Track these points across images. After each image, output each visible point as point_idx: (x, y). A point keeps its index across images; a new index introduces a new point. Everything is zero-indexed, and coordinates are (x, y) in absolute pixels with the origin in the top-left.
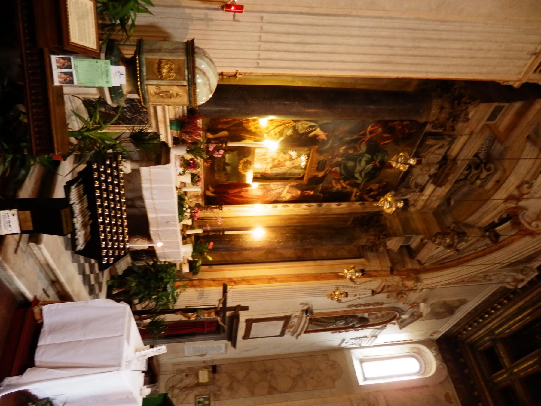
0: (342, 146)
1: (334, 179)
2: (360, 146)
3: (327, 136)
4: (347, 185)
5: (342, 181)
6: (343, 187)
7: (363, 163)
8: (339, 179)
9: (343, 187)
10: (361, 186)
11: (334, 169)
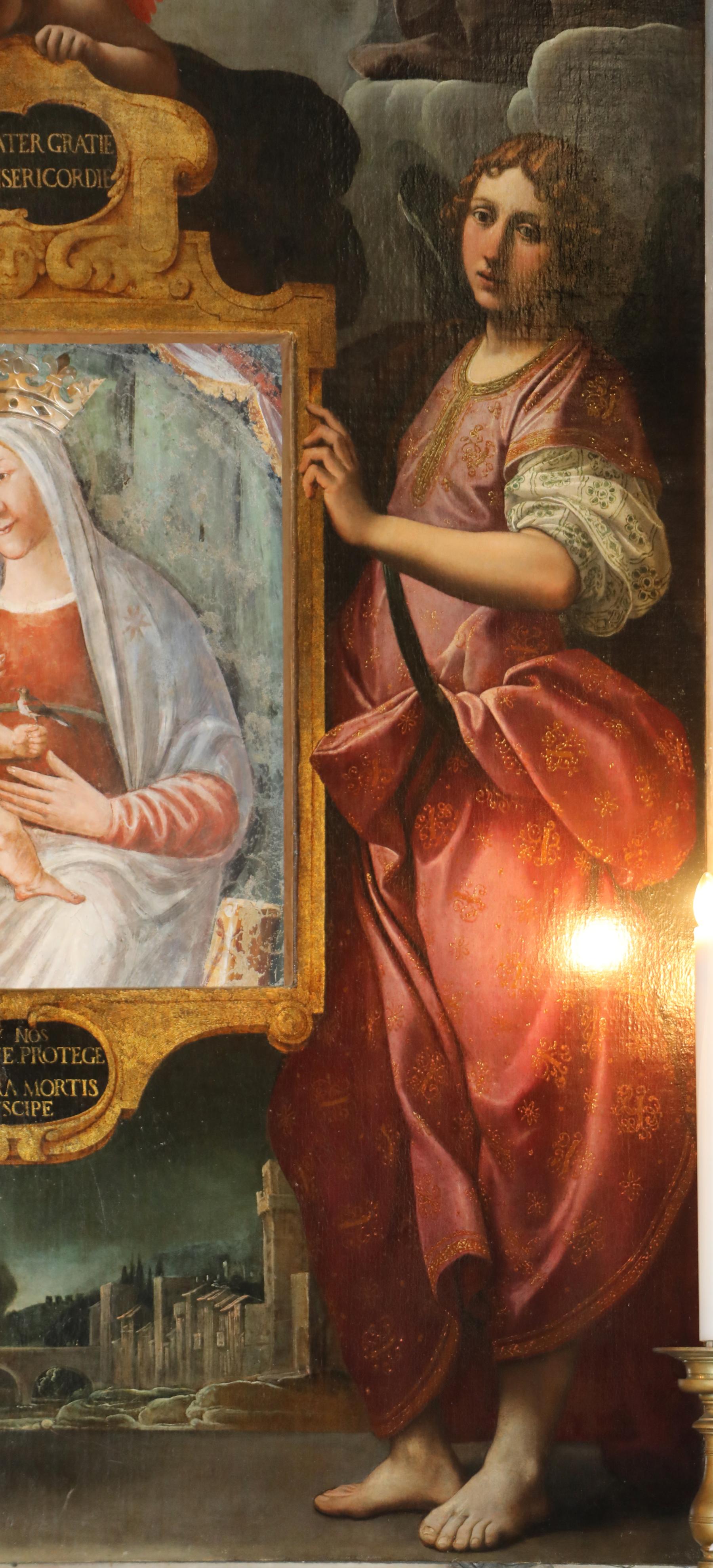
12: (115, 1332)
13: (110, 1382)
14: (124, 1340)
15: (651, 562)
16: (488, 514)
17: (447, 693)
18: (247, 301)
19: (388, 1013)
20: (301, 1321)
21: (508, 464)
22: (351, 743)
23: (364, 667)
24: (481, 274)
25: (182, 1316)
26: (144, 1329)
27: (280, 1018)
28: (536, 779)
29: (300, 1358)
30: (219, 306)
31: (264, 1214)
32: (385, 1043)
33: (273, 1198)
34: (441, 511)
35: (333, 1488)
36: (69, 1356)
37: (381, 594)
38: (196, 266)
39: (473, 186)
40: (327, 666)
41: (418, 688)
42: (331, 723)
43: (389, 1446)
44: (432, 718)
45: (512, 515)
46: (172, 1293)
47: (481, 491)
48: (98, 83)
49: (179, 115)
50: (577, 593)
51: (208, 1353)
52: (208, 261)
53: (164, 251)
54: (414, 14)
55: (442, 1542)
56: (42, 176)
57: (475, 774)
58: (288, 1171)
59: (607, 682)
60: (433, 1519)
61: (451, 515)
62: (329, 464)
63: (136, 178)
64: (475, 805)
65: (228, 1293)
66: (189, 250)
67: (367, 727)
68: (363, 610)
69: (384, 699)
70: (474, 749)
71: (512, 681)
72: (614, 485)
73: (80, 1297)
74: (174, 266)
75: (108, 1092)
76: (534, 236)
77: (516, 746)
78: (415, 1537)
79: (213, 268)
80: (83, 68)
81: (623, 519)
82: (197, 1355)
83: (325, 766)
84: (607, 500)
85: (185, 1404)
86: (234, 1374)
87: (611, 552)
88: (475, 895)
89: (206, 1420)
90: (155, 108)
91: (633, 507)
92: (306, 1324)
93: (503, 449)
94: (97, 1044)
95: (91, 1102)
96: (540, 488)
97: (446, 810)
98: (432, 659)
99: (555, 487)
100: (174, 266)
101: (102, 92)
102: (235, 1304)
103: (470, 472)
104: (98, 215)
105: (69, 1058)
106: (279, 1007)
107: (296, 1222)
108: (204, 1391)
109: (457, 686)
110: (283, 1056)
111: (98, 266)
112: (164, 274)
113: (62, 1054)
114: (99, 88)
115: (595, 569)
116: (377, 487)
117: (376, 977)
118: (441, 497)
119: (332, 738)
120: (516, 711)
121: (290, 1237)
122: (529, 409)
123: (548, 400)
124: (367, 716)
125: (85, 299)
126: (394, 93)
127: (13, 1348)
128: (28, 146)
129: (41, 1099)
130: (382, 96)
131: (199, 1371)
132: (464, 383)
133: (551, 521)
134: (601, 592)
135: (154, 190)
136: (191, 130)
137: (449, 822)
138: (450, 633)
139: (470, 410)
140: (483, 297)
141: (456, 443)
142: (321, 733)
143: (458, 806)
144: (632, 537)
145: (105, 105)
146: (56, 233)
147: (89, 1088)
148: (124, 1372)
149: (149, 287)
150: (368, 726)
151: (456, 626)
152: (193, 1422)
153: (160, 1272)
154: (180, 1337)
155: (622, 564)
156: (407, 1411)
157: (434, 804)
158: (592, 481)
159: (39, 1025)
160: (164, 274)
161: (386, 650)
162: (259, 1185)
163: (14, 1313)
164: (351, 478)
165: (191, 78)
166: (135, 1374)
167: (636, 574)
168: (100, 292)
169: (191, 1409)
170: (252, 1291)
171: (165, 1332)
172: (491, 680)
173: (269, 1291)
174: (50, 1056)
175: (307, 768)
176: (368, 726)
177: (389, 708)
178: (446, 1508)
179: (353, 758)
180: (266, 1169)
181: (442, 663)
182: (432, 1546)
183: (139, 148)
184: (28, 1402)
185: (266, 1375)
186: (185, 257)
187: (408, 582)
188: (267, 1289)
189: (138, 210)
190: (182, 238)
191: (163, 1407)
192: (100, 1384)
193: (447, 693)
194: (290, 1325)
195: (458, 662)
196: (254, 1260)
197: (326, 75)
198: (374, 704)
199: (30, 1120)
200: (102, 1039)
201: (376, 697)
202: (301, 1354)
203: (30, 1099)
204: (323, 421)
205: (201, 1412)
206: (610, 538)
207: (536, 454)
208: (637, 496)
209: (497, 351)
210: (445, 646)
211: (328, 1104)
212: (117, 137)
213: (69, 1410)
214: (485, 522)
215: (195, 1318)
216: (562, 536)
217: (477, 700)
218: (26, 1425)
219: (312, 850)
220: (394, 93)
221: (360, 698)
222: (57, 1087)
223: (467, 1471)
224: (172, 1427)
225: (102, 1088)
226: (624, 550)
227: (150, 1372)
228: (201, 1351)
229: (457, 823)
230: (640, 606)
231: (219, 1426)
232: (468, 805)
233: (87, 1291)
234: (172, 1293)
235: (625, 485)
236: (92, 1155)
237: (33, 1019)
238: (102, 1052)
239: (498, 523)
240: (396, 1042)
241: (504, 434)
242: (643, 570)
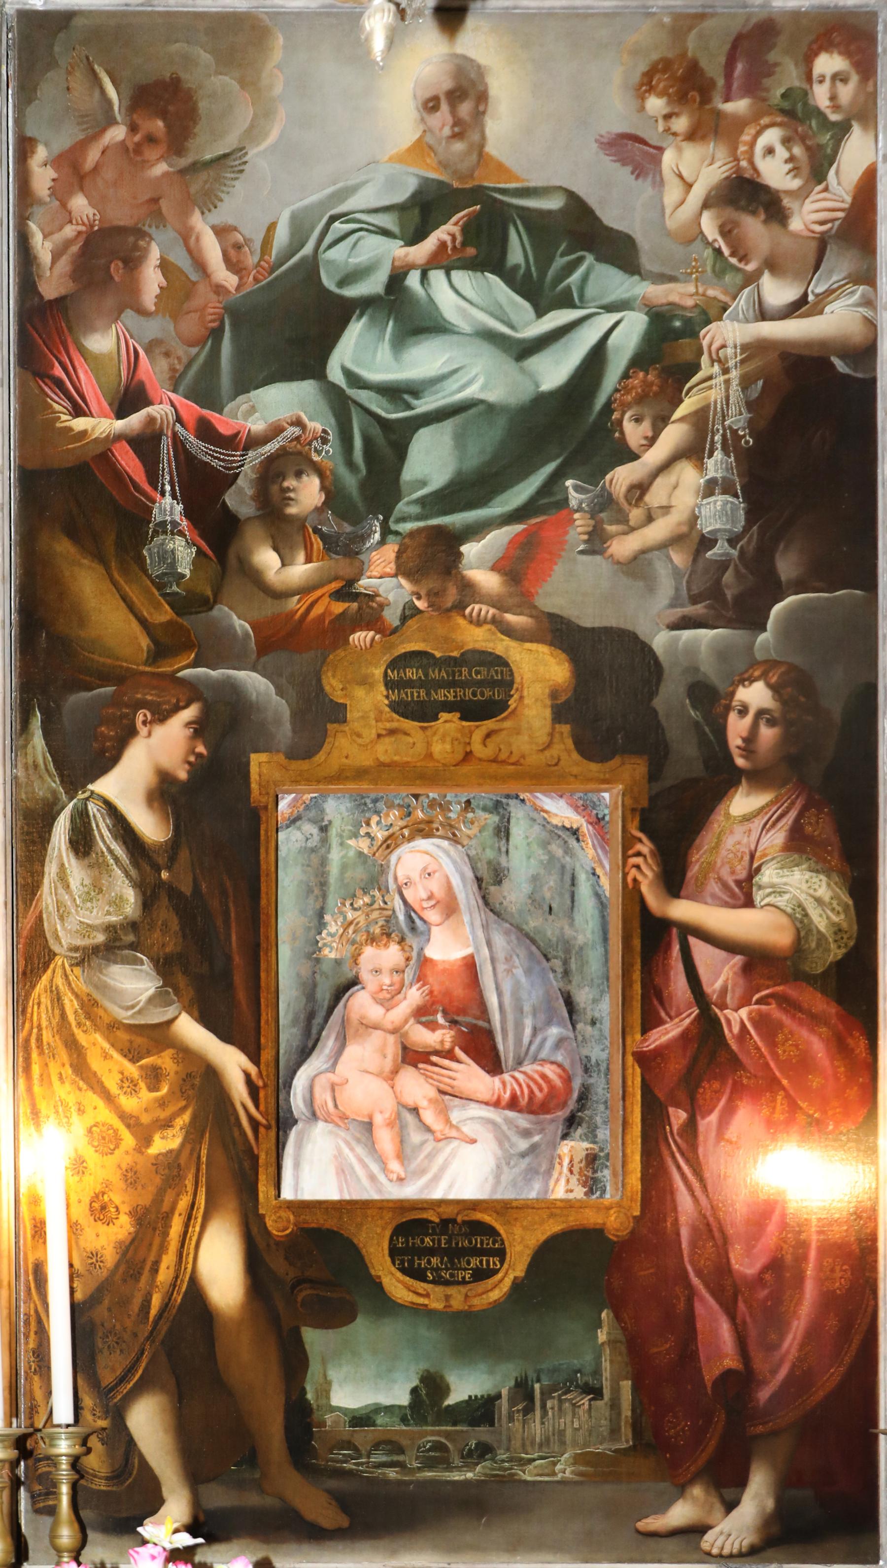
0: (254, 577)
1: (596, 542)
2: (254, 442)
3: (161, 716)
4: (661, 422)
5: (622, 477)
6: (694, 451)
7: (424, 360)
8: (605, 503)
9: (694, 451)
10: (680, 294)
11: (487, 580)
12: (511, 1419)
13: (508, 1450)
14: (516, 1423)
15: (845, 925)
16: (742, 898)
17: (717, 1011)
18: (594, 767)
19: (680, 1215)
20: (626, 1412)
21: (755, 865)
22: (657, 1043)
23: (665, 994)
24: (739, 747)
25: (552, 1408)
26: (529, 1416)
27: (613, 1218)
28: (772, 1064)
29: (626, 1435)
30: (575, 770)
31: (603, 1344)
32: (678, 1234)
33: (609, 1333)
34: (714, 896)
35: (646, 1517)
36: (482, 1433)
37: (676, 949)
38: (562, 746)
39: (732, 694)
40: (643, 995)
41: (699, 1008)
42: (645, 1030)
43: (681, 1490)
44: (708, 1025)
45: (758, 897)
46: (546, 1394)
47: (738, 883)
48: (503, 637)
49: (552, 655)
50: (799, 948)
51: (569, 1432)
52: (570, 743)
53: (542, 737)
54: (695, 591)
55: (715, 1551)
56: (469, 692)
57: (735, 1062)
58: (617, 1316)
59: (818, 1002)
60: (709, 1536)
61: (719, 898)
62: (644, 867)
63: (525, 693)
64: (735, 1083)
65: (581, 1393)
66: (557, 735)
67: (667, 1033)
68: (665, 959)
69: (677, 1016)
70: (734, 1046)
71: (758, 1002)
72: (822, 877)
73: (489, 1395)
74: (548, 746)
75: (506, 1266)
76: (771, 723)
77: (760, 1044)
78: (698, 1548)
79: (572, 747)
80: (493, 628)
81: (827, 899)
82: (562, 1433)
83: (642, 1058)
84: (816, 887)
85: (555, 1464)
86: (586, 1445)
87: (820, 920)
88: (734, 1139)
89: (568, 1474)
90: (537, 651)
91: (833, 891)
92: (629, 1413)
93: (752, 857)
94: (499, 1235)
95: (496, 1272)
96: (776, 880)
97: (716, 1085)
98: (708, 989)
99: (784, 880)
100: (548, 746)
101: (505, 643)
102: (585, 1401)
103: (731, 871)
104: (503, 715)
105: (482, 1243)
106: (612, 1212)
107: (623, 1348)
108: (566, 1456)
109: (723, 1006)
110: (615, 1243)
111: (502, 747)
112: (542, 751)
113: (477, 1241)
114: (502, 640)
115: (810, 930)
116: (674, 882)
117: (672, 1192)
118: (714, 887)
119: (645, 1040)
120: (760, 1021)
121: (619, 1358)
122: (768, 831)
123: (780, 825)
124: (667, 1026)
125: (494, 765)
126: (684, 638)
127: (449, 1428)
128: (461, 675)
129: (465, 1269)
130: (678, 639)
131: (563, 1443)
132: (728, 815)
133: (781, 901)
134: (813, 945)
135: (537, 700)
136: (558, 664)
137: (718, 1093)
138: (718, 972)
139: (732, 832)
140: (740, 762)
141: (723, 853)
142: (638, 1037)
143: (723, 1083)
144: (833, 910)
145: (507, 649)
146: (477, 727)
147: (494, 1263)
148: (516, 1443)
149: (535, 759)
150: (667, 1033)
151: (723, 968)
152: (560, 1475)
153: (538, 1381)
154: (551, 1422)
155: (826, 927)
156: (693, 1469)
157: (709, 1081)
158: (808, 875)
159: (464, 1222)
160: (542, 751)
161: (679, 984)
162: (599, 1325)
163: (449, 1406)
164: (657, 876)
165: (559, 632)
166: (523, 1445)
167: (835, 933)
168: (503, 762)
169: (558, 1467)
170: (596, 1392)
171: (542, 1418)
172: (745, 1002)
173: (607, 1393)
174: (470, 1242)
175: (630, 1059)
176: (667, 1033)
177: (681, 1021)
178: (717, 1530)
179: (659, 1053)
180: (604, 1315)
181: (714, 991)
182: (709, 1554)
183: (527, 676)
184: (457, 1462)
185: (605, 1446)
186: (555, 740)
187: (692, 940)
188: (605, 1391)
189: (527, 712)
190: (553, 729)
191: (541, 1465)
192: (502, 1451)
193: (717, 1011)
194: (619, 1414)
195: (724, 991)
196: (597, 1372)
197: (642, 630)
198: (671, 1018)
199: (458, 1283)
200: (502, 1232)
201: (673, 1013)
202: (626, 1432)
203: (458, 1269)
204: (640, 841)
205: (565, 1469)
206: (819, 911)
207: (773, 859)
208: (836, 884)
209: (748, 794)
210: (716, 981)
211: (642, 1273)
212: (514, 668)
213: (483, 1467)
214: (741, 902)
215: (560, 1409)
216: (789, 910)
217: (735, 1014)
218: (456, 1476)
219: (632, 1112)
220: (684, 638)
221: (663, 1014)
222: (474, 1262)
223: (730, 1506)
224: (547, 1479)
225: (502, 1262)
226: (828, 918)
227: (533, 1443)
228: (564, 1430)
229: (723, 1093)
230: (836, 953)
231: (577, 1478)
232: (730, 1081)
233: (493, 1393)
234: (546, 1394)
235: (828, 877)
236: (496, 1304)
237: (459, 1219)
238: (502, 1240)
239: (749, 903)
240: (685, 1233)
241: (753, 847)
242: (840, 930)
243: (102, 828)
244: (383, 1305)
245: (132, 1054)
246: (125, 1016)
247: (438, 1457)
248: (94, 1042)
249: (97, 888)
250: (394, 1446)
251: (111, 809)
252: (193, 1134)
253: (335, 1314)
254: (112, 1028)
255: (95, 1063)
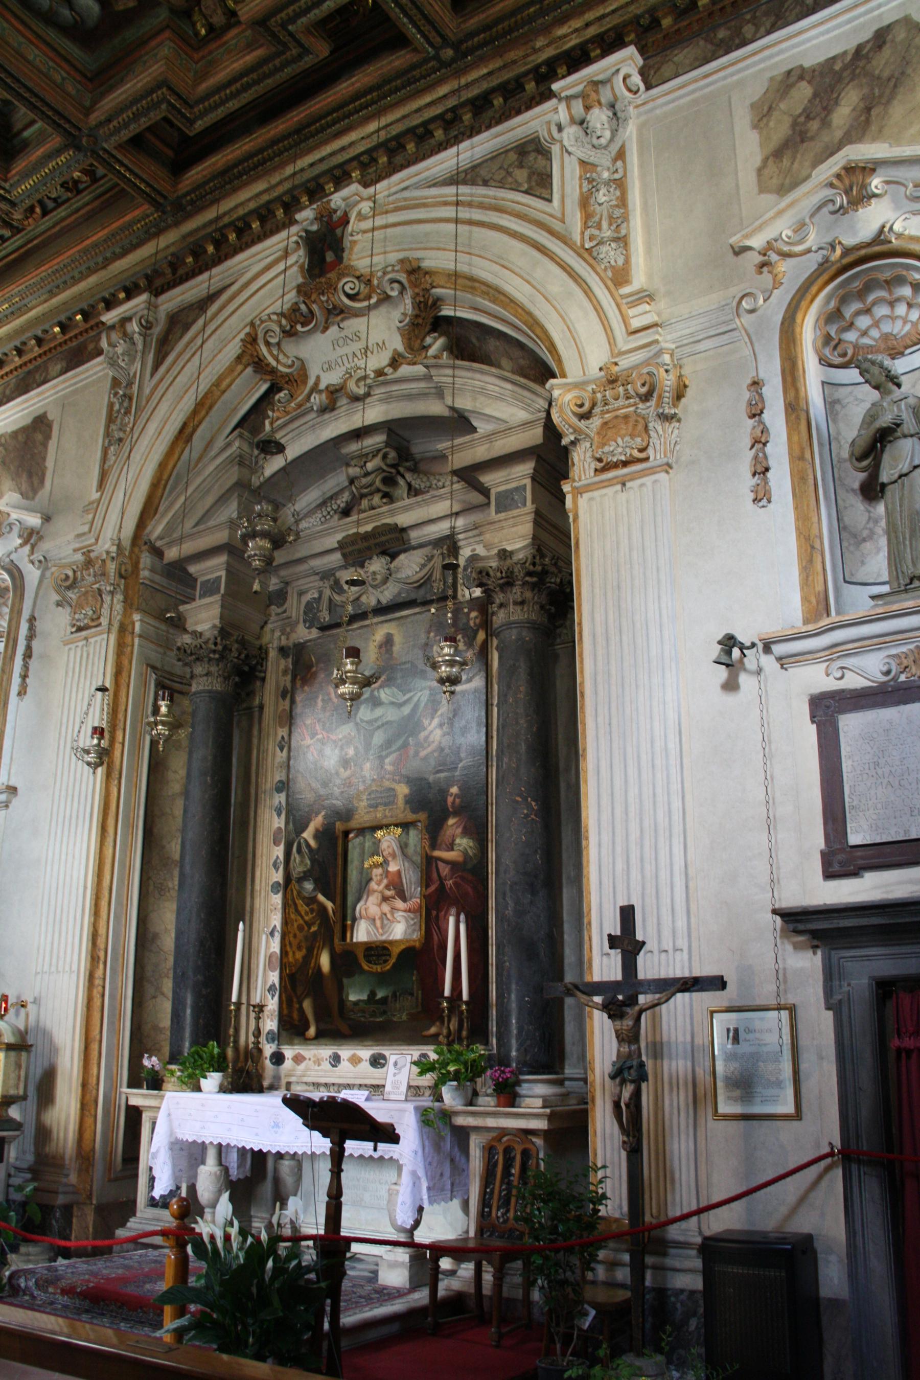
50: (465, 862)
116: (434, 846)
120: (455, 883)
138: (445, 870)
150: (433, 888)
161: (435, 875)
205: (404, 1017)
239: (452, 850)
243: (303, 845)
244: (362, 971)
245: (307, 905)
246: (307, 895)
247: (374, 1014)
248: (300, 902)
249: (302, 862)
250: (363, 1011)
251: (306, 841)
252: (320, 926)
253: (350, 974)
254: (303, 898)
255: (300, 908)
